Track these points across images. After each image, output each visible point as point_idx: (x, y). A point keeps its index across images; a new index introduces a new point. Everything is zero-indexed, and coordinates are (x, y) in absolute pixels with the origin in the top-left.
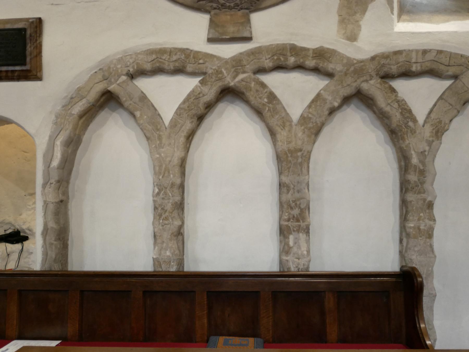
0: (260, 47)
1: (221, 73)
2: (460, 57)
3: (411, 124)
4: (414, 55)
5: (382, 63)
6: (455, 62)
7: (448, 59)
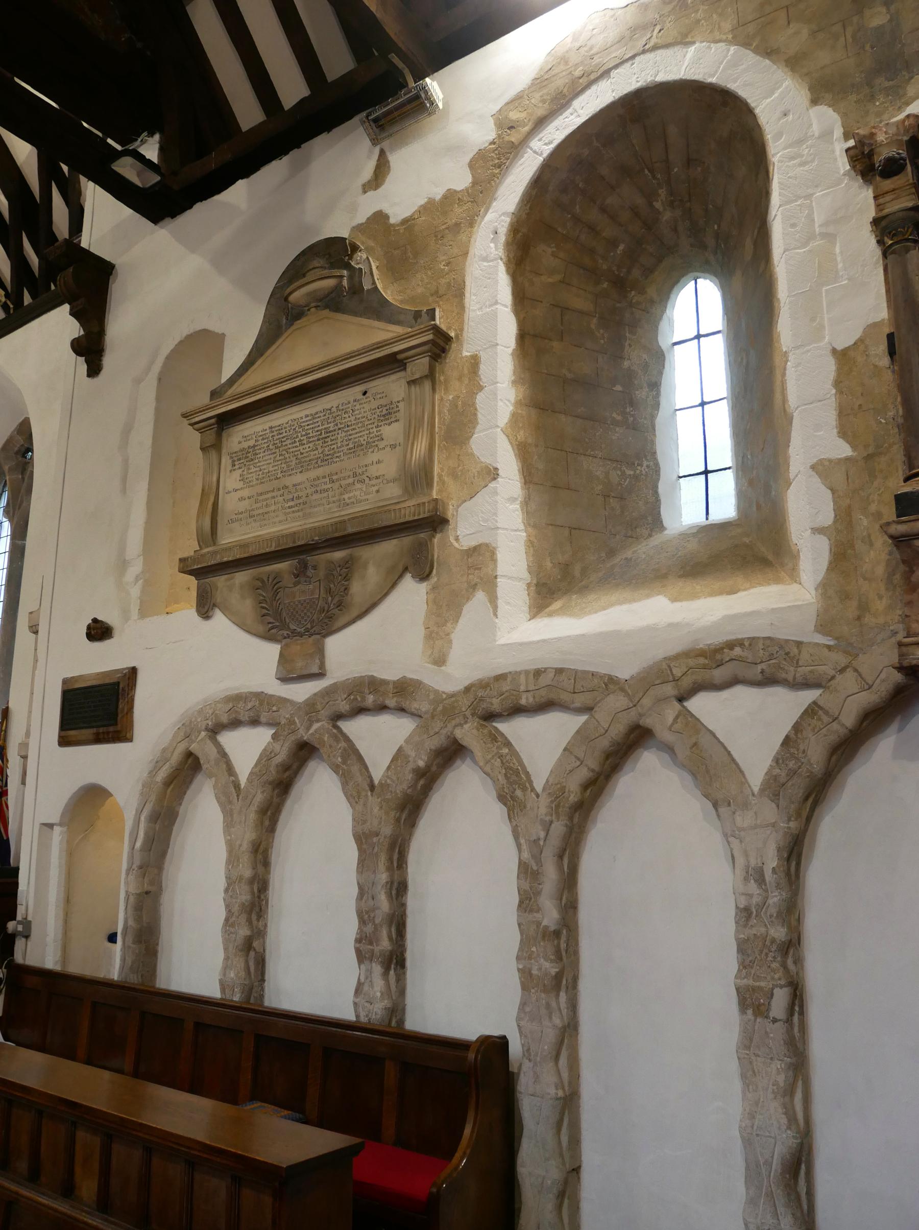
0: (335, 684)
1: (294, 723)
2: (590, 676)
3: (519, 793)
4: (522, 679)
5: (480, 696)
6: (582, 686)
7: (573, 681)
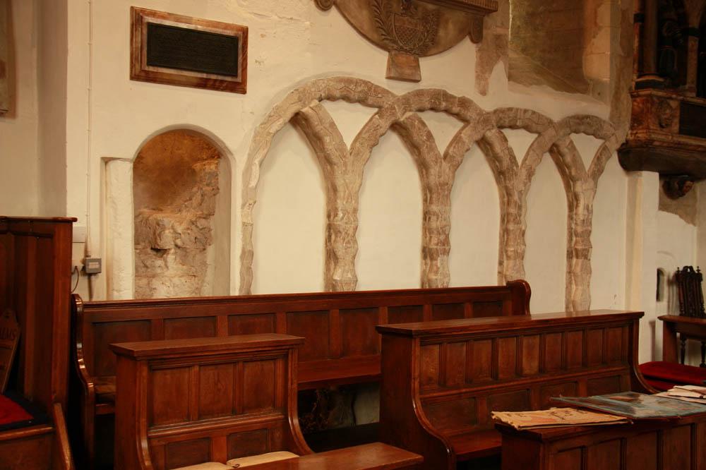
1: (394, 108)
3: (515, 168)
